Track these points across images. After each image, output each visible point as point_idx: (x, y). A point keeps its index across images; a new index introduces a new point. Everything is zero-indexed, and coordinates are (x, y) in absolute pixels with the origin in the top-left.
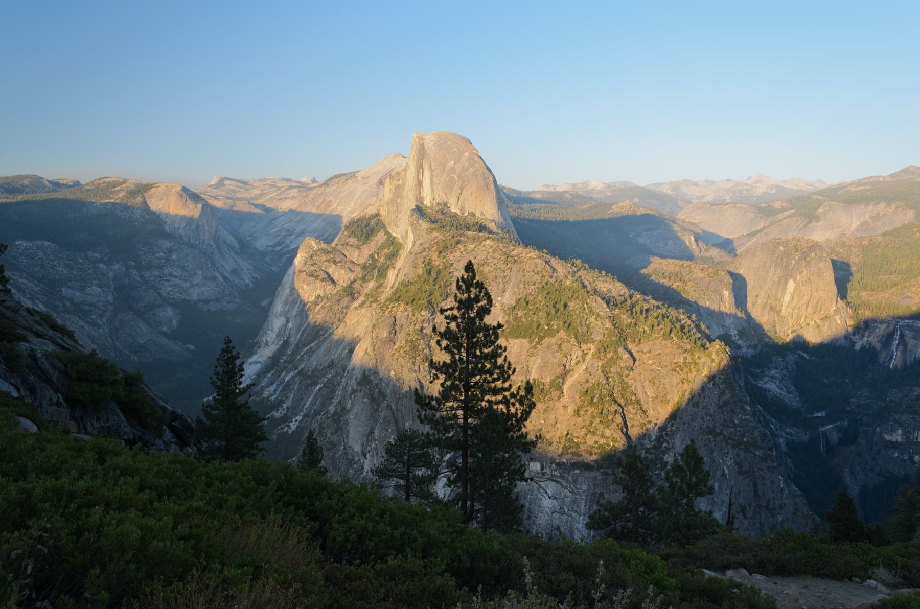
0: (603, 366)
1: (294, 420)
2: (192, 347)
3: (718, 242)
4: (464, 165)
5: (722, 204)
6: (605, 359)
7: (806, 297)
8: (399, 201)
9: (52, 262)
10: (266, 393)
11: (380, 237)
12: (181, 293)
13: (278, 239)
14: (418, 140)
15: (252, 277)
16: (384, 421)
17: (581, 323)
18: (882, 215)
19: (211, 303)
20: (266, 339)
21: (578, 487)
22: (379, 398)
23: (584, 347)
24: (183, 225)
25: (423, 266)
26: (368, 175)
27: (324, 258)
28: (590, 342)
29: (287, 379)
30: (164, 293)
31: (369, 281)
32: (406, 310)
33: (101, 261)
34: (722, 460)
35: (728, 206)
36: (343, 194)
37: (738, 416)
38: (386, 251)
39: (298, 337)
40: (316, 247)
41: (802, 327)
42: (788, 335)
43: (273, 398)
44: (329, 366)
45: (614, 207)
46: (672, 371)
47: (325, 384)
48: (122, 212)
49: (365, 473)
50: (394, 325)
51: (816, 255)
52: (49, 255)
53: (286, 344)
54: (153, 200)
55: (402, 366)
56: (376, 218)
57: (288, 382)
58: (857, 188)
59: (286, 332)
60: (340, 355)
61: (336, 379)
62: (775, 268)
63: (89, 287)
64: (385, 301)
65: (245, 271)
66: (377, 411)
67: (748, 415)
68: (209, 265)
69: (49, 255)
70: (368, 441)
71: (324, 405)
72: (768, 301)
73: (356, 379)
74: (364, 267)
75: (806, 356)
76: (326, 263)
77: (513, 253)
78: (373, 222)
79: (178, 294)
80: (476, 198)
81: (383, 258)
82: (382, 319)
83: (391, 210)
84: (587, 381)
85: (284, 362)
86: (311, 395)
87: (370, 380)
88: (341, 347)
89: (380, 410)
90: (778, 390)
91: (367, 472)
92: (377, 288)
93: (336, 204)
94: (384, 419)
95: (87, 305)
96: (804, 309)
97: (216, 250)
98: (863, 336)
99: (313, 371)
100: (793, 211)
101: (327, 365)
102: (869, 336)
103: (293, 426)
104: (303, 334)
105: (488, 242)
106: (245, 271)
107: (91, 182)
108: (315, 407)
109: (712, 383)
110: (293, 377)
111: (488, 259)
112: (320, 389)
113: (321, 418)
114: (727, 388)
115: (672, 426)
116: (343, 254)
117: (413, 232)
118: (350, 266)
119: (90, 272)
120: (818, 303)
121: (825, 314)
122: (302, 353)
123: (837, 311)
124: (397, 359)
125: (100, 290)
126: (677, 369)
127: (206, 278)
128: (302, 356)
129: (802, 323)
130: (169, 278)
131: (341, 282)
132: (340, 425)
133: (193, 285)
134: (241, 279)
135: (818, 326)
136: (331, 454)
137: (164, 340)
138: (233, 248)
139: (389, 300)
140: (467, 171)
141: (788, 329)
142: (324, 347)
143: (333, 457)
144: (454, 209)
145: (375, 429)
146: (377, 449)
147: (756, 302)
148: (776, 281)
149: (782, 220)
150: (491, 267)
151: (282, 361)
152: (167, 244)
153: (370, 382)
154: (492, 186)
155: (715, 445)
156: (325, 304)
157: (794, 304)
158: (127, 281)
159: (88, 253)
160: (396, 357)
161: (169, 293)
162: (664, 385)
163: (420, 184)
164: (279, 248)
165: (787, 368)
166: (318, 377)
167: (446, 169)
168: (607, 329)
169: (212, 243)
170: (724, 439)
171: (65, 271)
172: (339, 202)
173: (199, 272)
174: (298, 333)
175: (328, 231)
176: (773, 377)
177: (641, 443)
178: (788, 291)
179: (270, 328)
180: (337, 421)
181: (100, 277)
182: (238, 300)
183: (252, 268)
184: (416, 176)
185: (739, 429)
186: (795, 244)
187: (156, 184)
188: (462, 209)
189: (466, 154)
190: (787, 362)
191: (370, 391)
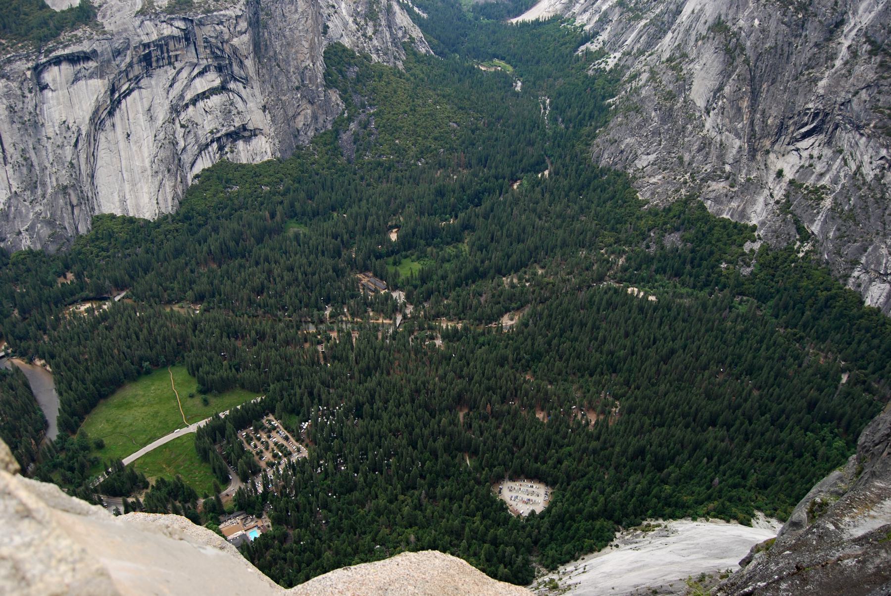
1: (612, 56)
10: (578, 23)
29: (604, 8)
43: (587, 28)
49: (705, 132)
55: (770, 15)
57: (606, 14)
61: (666, 16)
70: (714, 97)
73: (705, 23)
86: (633, 31)
87: (726, 26)
94: (739, 76)
103: (611, 63)
108: (639, 45)
112: (645, 26)
124: (765, 5)
132: (682, 73)
136: (668, 105)
143: (671, 109)
153: (727, 29)
180: (677, 68)
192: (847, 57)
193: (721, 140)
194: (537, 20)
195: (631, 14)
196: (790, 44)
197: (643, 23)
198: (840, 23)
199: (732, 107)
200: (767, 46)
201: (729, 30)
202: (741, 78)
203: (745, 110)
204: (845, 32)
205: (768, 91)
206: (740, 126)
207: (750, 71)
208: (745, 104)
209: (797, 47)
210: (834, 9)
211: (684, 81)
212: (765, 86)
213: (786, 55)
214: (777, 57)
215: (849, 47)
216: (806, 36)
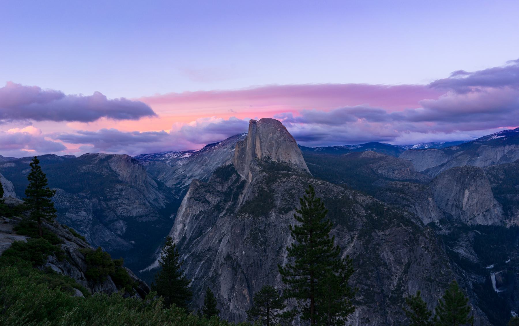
0: (363, 245)
2: (133, 242)
3: (423, 171)
5: (423, 150)
6: (365, 240)
7: (476, 199)
8: (243, 157)
9: (61, 199)
11: (234, 177)
12: (128, 213)
13: (178, 181)
14: (252, 124)
15: (165, 202)
16: (240, 281)
17: (349, 219)
18: (514, 151)
19: (143, 218)
20: (173, 236)
21: (354, 315)
22: (237, 267)
23: (352, 233)
24: (128, 176)
25: (258, 191)
27: (204, 190)
28: (355, 231)
29: (185, 258)
30: (119, 214)
31: (229, 201)
32: (250, 217)
33: (86, 197)
34: (437, 296)
35: (427, 150)
36: (212, 155)
37: (443, 269)
38: (237, 184)
39: (191, 234)
40: (199, 184)
41: (476, 216)
42: (468, 221)
44: (208, 250)
45: (363, 154)
46: (404, 245)
47: (206, 260)
48: (96, 171)
49: (230, 311)
50: (244, 226)
51: (479, 175)
52: (60, 196)
53: (184, 238)
54: (113, 164)
55: (249, 249)
56: (231, 167)
58: (498, 137)
59: (185, 232)
60: (214, 243)
62: (456, 183)
63: (80, 212)
64: (238, 212)
65: (161, 199)
66: (236, 275)
67: (449, 268)
68: (142, 197)
69: (60, 196)
70: (231, 292)
71: (206, 273)
72: (455, 202)
73: (224, 257)
74: (225, 194)
75: (479, 233)
76: (205, 193)
77: (308, 182)
78: (229, 169)
79: (126, 213)
80: (286, 153)
81: (236, 188)
82: (237, 222)
83: (239, 162)
84: (355, 253)
85: (183, 249)
86: (199, 267)
87: (231, 257)
88: (214, 239)
89: (238, 274)
90: (465, 253)
91: (232, 310)
92: (233, 205)
93: (209, 160)
94: (240, 279)
95: (78, 221)
96: (475, 206)
97: (146, 188)
98: (511, 220)
99: (200, 253)
100: (464, 151)
101: (207, 250)
102: (514, 220)
104: (193, 233)
105: (294, 176)
106: (161, 199)
107: (81, 156)
109: (427, 251)
110: (188, 257)
111: (294, 186)
112: (204, 263)
113: (205, 280)
114: (436, 253)
115: (406, 277)
116: (214, 187)
117: (252, 173)
118: (218, 194)
119: (80, 203)
120: (483, 202)
121: (488, 208)
122: (193, 243)
123: (494, 206)
124: (246, 245)
125: (85, 213)
126: (406, 244)
127: (140, 204)
128: (193, 245)
129: (475, 214)
130: (121, 205)
131: (213, 203)
133: (133, 208)
134: (159, 203)
135: (484, 216)
137: (119, 239)
138: (154, 187)
139: (241, 211)
141: (468, 218)
142: (205, 239)
144: (274, 160)
145: (235, 285)
146: (237, 297)
147: (448, 203)
148: (458, 191)
149: (458, 157)
150: (296, 190)
151: (182, 248)
152: (120, 187)
153: (231, 258)
155: (432, 287)
156: (204, 215)
157: (470, 203)
158: (99, 208)
159: (79, 193)
160: (245, 243)
161: (121, 213)
162: (400, 253)
163: (254, 147)
164: (179, 186)
165: (469, 240)
166: (202, 256)
168: (364, 222)
169: (143, 185)
170: (437, 283)
171: (68, 204)
172: (210, 159)
173: (137, 201)
174: (191, 232)
175: (205, 175)
176: (461, 246)
177: (388, 288)
178: (465, 196)
179: (175, 230)
180: (214, 281)
181: (86, 206)
182: (157, 215)
183: (165, 197)
185: (445, 277)
186: (466, 169)
187: (114, 155)
189: (279, 129)
190: (469, 237)
191: (232, 263)
192: (287, 261)
193: (239, 314)
194: (153, 269)
195: (197, 259)
196: (261, 260)
197: (202, 263)
198: (281, 248)
199: (240, 295)
200: (250, 263)
201: (232, 258)
202: (241, 280)
203: (247, 296)
204: (284, 251)
205: (255, 284)
206: (246, 304)
207: (246, 277)
208: (245, 292)
209: (264, 261)
210: (277, 242)
211: (217, 287)
212: (253, 282)
213: (260, 265)
214: (256, 267)
215: (287, 257)
216: (267, 255)
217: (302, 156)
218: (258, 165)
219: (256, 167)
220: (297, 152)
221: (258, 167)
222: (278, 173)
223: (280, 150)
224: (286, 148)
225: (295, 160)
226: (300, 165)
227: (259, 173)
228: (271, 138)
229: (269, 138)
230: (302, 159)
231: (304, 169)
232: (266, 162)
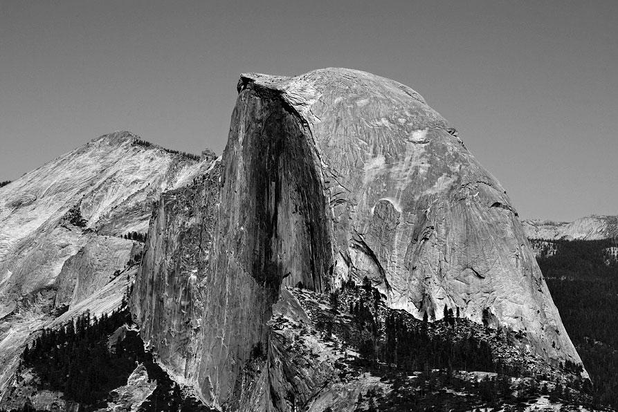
4: (416, 169)
8: (193, 277)
11: (138, 387)
26: (33, 197)
78: (111, 342)
83: (168, 303)
140: (431, 185)
144: (400, 302)
154: (510, 233)
163: (266, 225)
167: (365, 181)
184: (252, 203)
188: (424, 302)
189: (418, 135)
217: (545, 287)
218: (320, 326)
219: (311, 341)
220: (524, 264)
221: (327, 339)
222: (449, 381)
223: (432, 252)
224: (466, 243)
225: (519, 311)
226: (544, 336)
227: (342, 376)
228: (376, 181)
229: (366, 180)
230: (553, 311)
231: (568, 363)
232: (361, 314)
